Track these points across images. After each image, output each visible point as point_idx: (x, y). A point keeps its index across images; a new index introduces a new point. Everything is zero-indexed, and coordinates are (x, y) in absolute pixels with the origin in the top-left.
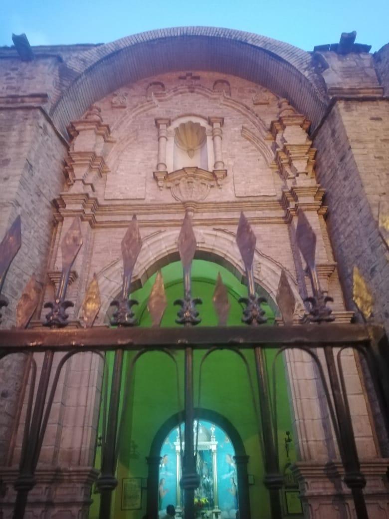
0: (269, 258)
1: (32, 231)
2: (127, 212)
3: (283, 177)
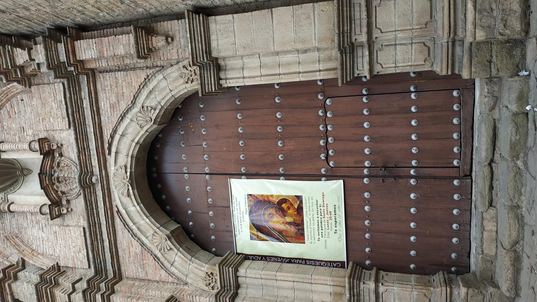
0: (136, 96)
2: (100, 246)
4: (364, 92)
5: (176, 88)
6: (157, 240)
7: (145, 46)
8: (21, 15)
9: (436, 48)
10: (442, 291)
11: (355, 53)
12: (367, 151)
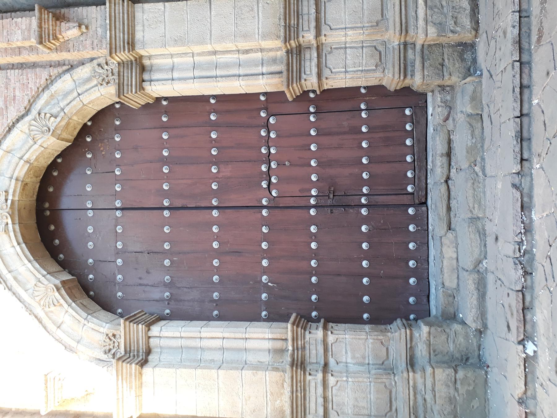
0: (32, 101)
4: (312, 110)
5: (86, 91)
7: (51, 32)
9: (387, 53)
10: (400, 334)
11: (303, 56)
12: (314, 178)
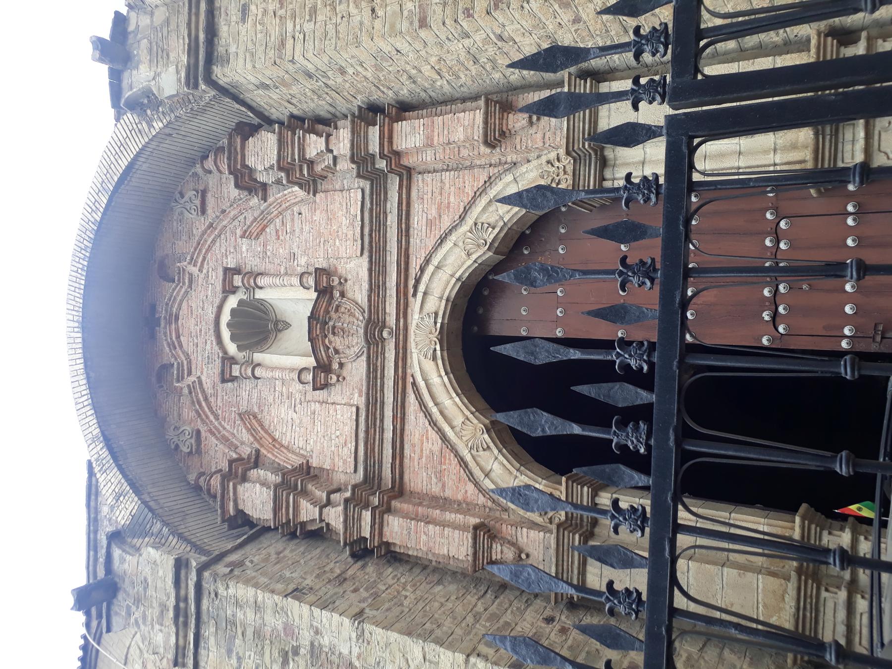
1: (404, 593)
3: (330, 175)
4: (850, 208)
6: (467, 433)
8: (330, 83)
11: (841, 136)
